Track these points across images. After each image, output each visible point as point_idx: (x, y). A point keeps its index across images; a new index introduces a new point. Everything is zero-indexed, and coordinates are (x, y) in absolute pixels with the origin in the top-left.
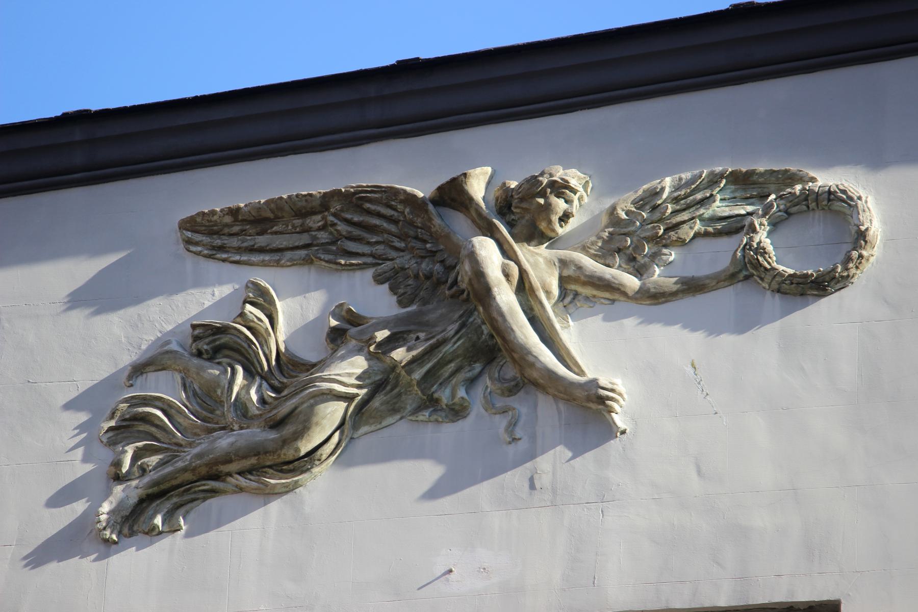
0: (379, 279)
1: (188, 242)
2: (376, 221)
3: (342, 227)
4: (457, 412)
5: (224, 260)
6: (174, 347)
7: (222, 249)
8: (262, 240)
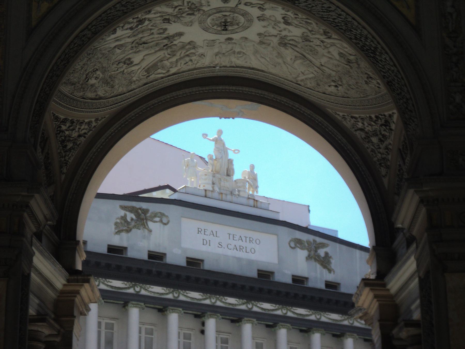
1: (120, 208)
4: (140, 229)
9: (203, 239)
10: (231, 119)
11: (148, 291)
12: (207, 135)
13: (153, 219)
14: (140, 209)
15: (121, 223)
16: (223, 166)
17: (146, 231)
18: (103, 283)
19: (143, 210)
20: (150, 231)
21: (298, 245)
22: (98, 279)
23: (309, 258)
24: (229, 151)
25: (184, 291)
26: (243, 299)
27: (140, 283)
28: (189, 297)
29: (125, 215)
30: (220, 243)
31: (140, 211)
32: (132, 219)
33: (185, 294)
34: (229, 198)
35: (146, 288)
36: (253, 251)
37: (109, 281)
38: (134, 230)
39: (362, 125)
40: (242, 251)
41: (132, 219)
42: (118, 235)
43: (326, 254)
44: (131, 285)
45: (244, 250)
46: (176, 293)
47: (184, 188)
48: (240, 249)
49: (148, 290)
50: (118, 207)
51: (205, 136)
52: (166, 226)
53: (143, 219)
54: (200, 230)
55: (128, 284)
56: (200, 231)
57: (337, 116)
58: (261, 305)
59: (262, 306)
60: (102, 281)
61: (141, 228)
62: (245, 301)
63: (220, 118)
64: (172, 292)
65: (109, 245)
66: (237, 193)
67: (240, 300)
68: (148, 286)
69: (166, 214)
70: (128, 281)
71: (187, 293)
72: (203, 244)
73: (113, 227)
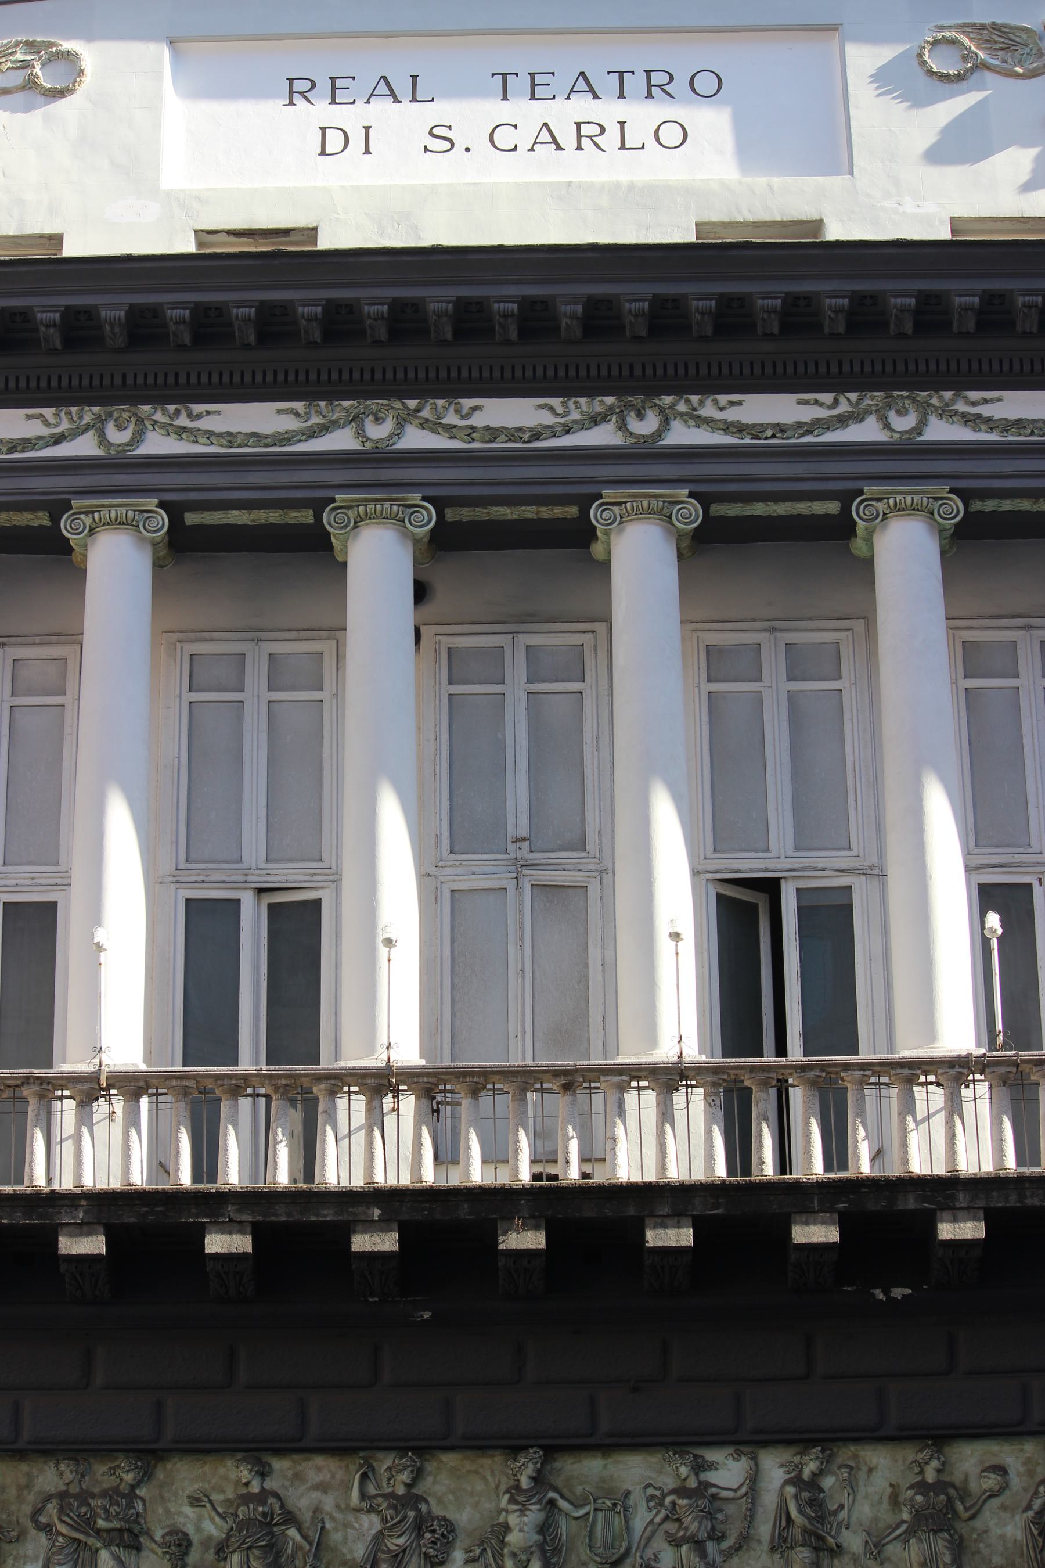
25: (172, 408)
33: (183, 421)
46: (120, 428)
58: (721, 409)
59: (732, 415)
64: (98, 426)
67: (571, 403)
71: (199, 416)
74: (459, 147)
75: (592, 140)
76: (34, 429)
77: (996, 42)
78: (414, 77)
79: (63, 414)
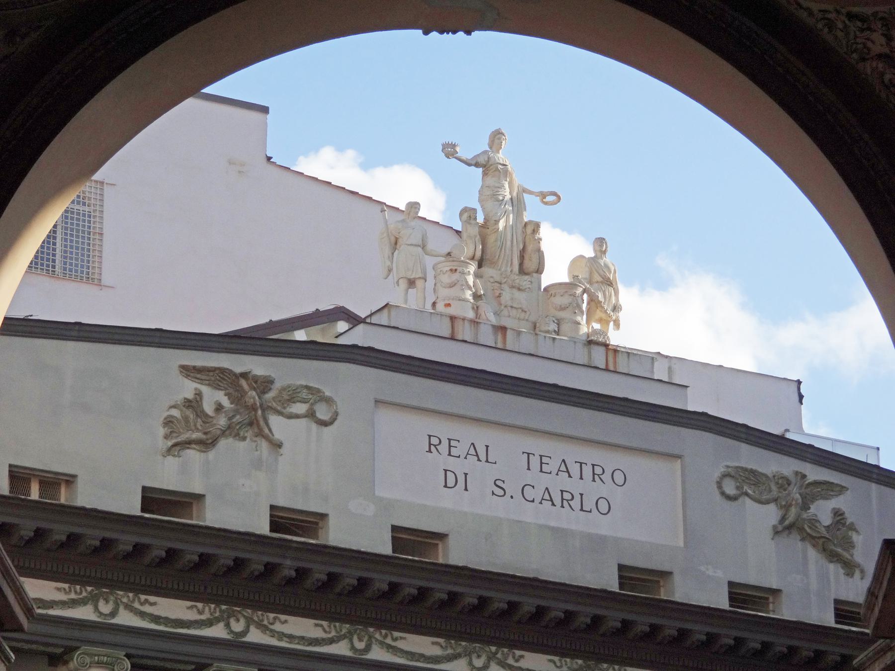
0: (226, 395)
1: (181, 372)
2: (226, 378)
3: (218, 377)
4: (244, 439)
5: (189, 379)
6: (179, 403)
7: (189, 376)
8: (199, 376)
9: (446, 471)
10: (461, 34)
11: (272, 631)
12: (454, 146)
13: (285, 408)
14: (244, 375)
15: (186, 419)
16: (509, 243)
17: (264, 444)
18: (129, 607)
19: (256, 379)
20: (279, 445)
21: (746, 488)
22: (111, 594)
23: (784, 529)
24: (526, 196)
25: (384, 632)
26: (573, 657)
27: (245, 606)
28: (401, 651)
29: (199, 394)
30: (498, 483)
31: (243, 382)
32: (219, 408)
33: (389, 641)
34: (527, 343)
35: (265, 622)
36: (603, 506)
37: (146, 601)
38: (223, 443)
39: (883, 40)
40: (569, 504)
41: (219, 408)
42: (174, 456)
43: (838, 514)
44: (217, 614)
45: (576, 504)
46: (360, 640)
47: (385, 311)
48: (563, 499)
49: (272, 627)
50: (176, 371)
51: (450, 151)
52: (326, 430)
53: (254, 408)
54: (434, 441)
55: (207, 611)
56: (435, 446)
57: (804, 15)
60: (125, 600)
61: (249, 434)
62: (580, 662)
63: (426, 33)
64: (349, 636)
65: (145, 489)
66: (553, 327)
68: (272, 615)
69: (327, 393)
70: (206, 600)
72: (446, 486)
73: (162, 431)
74: (508, 495)
75: (568, 502)
76: (318, 633)
77: (750, 479)
78: (487, 447)
79: (332, 626)
